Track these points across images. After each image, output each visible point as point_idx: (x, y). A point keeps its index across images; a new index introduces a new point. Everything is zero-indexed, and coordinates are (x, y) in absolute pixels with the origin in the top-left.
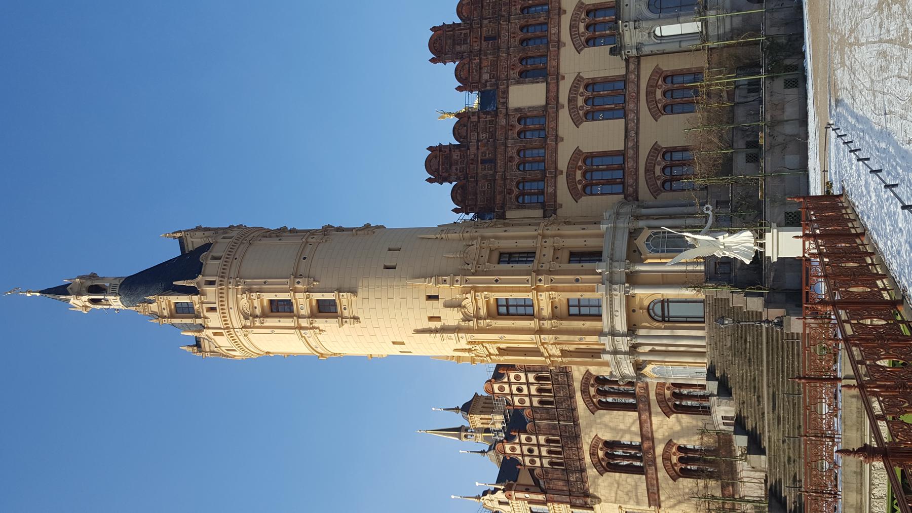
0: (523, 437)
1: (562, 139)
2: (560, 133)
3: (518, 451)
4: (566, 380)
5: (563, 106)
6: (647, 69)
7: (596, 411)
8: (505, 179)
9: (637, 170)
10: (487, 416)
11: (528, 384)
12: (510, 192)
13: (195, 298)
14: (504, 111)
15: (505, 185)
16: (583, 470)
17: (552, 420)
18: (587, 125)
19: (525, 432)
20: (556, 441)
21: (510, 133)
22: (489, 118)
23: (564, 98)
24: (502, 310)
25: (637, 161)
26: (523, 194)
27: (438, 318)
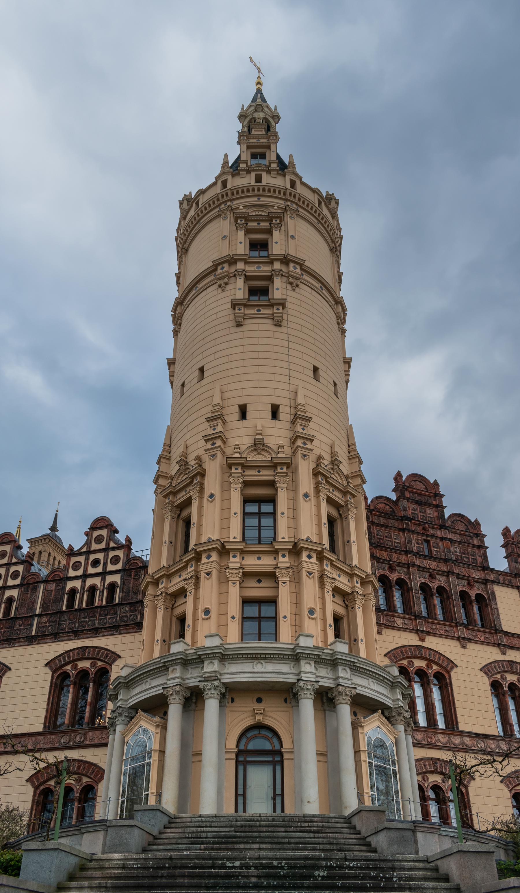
1: (464, 647)
2: (471, 646)
4: (107, 626)
5: (504, 653)
7: (51, 668)
8: (408, 566)
11: (104, 574)
12: (392, 569)
15: (400, 565)
17: (42, 606)
18: (485, 682)
21: (465, 582)
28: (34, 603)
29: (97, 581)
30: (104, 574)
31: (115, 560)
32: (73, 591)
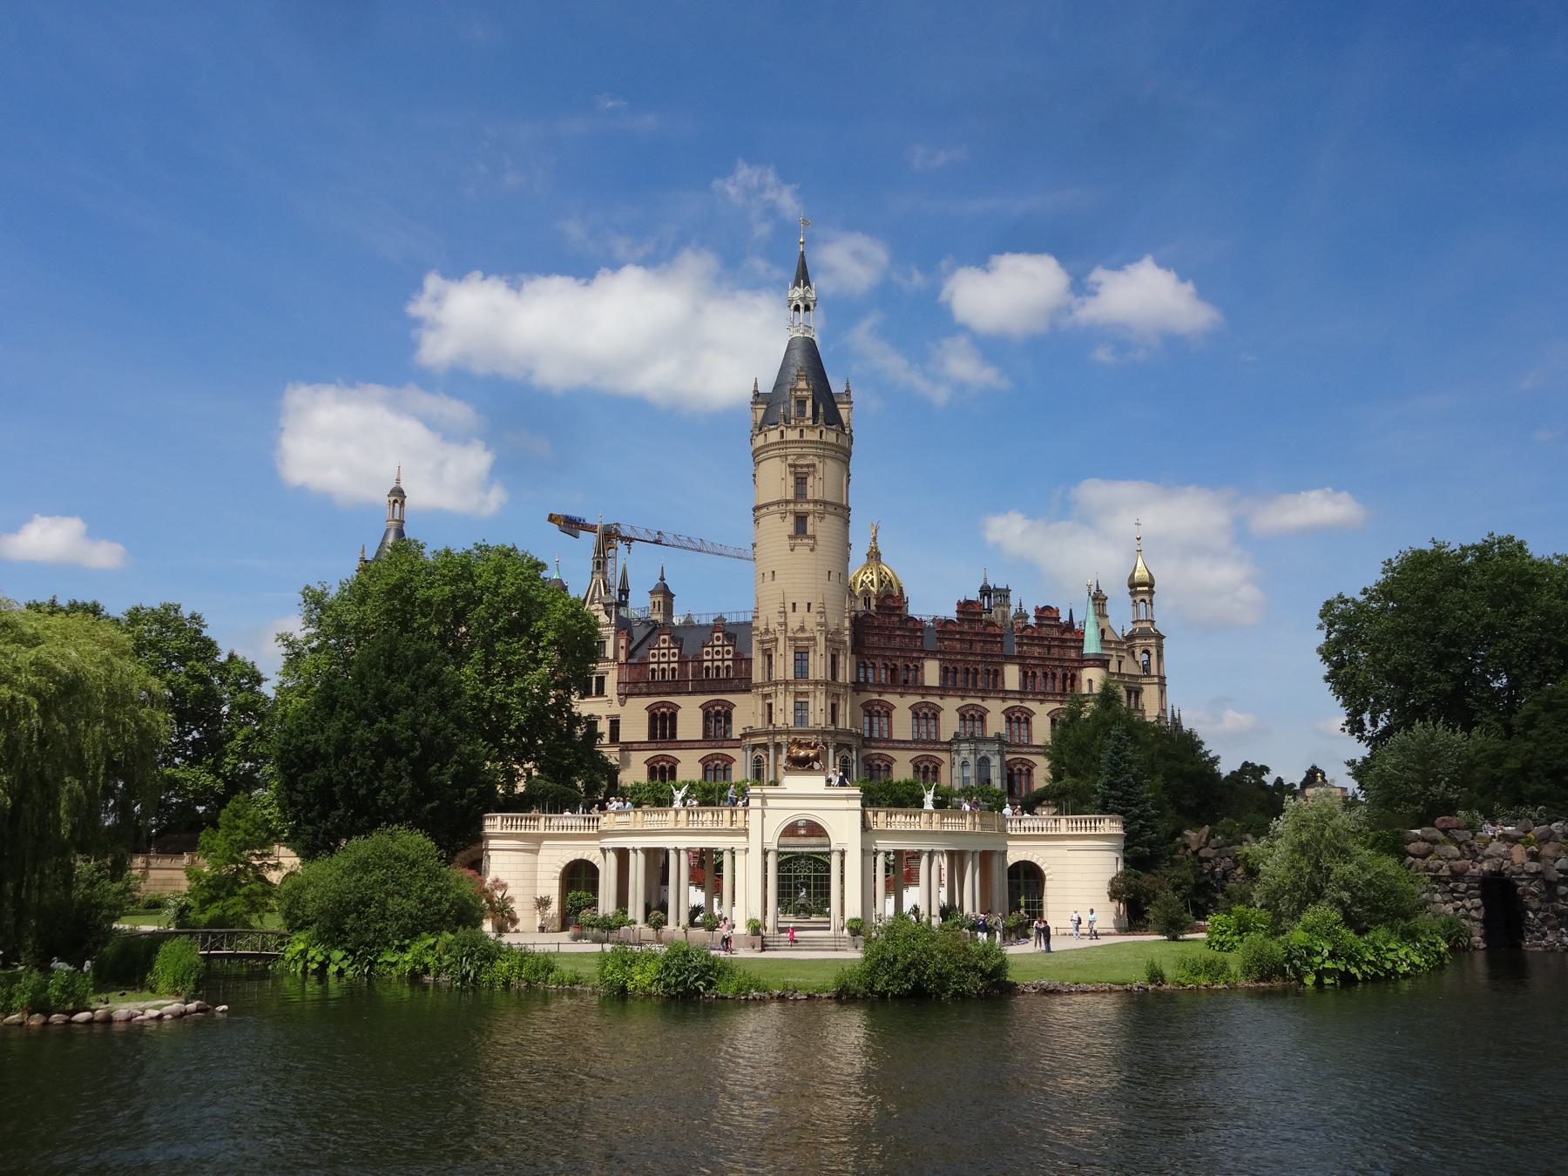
0: (676, 651)
3: (662, 645)
6: (944, 756)
9: (880, 748)
10: (662, 607)
13: (810, 422)
14: (923, 655)
16: (648, 694)
19: (680, 652)
20: (673, 676)
22: (919, 644)
23: (929, 699)
24: (801, 656)
25: (884, 748)
26: (866, 667)
27: (794, 610)
28: (687, 673)
29: (720, 663)
30: (723, 660)
31: (728, 653)
32: (707, 668)
